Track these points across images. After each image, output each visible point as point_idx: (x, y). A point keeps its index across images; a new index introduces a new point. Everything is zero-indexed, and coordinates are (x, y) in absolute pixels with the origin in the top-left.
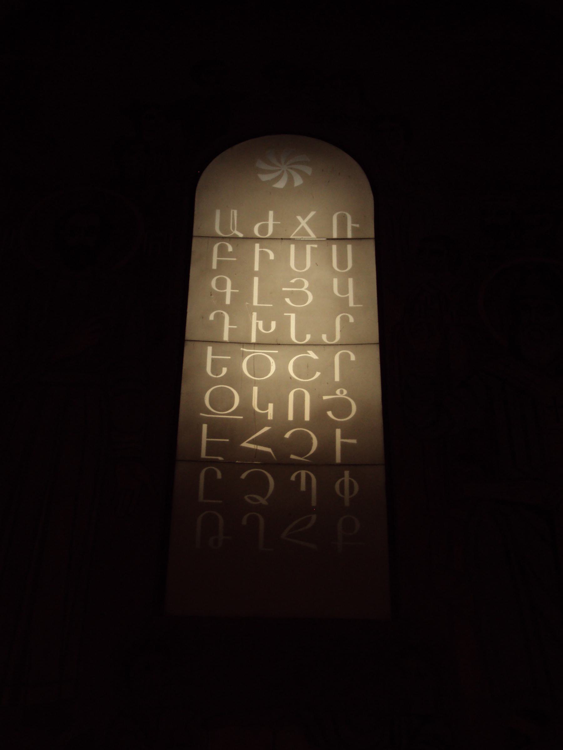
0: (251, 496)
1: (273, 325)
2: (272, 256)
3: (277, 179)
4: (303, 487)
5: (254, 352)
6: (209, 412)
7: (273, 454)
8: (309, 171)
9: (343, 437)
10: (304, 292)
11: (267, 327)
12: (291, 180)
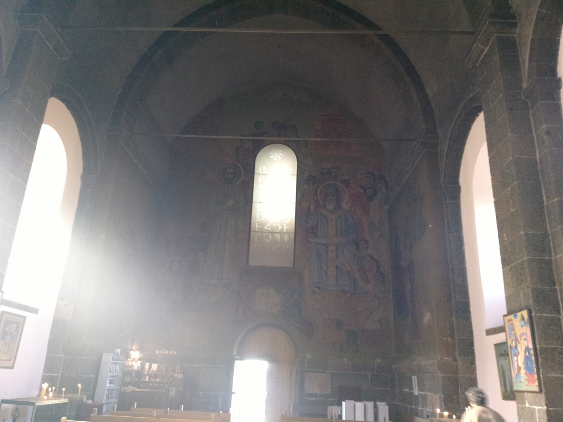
3: (275, 157)
6: (258, 220)
8: (282, 155)
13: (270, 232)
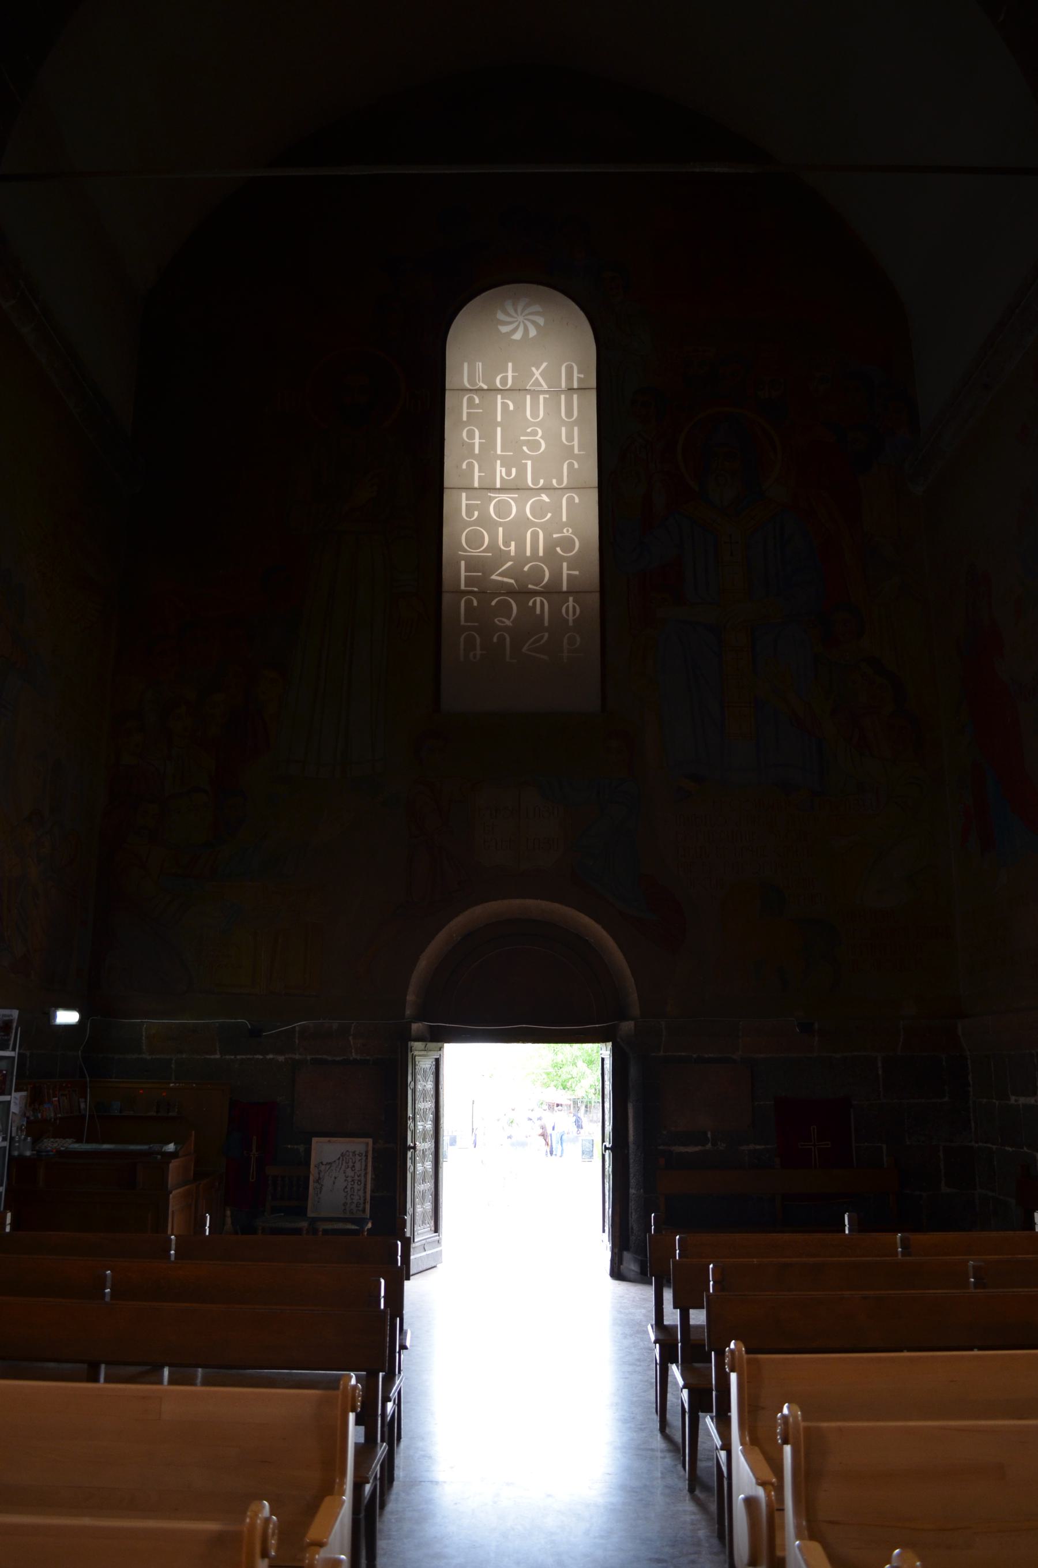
0: (500, 619)
1: (514, 471)
2: (511, 407)
3: (515, 330)
4: (538, 611)
5: (499, 497)
6: (466, 551)
7: (515, 584)
8: (541, 321)
9: (569, 569)
10: (538, 440)
11: (509, 474)
12: (526, 330)
13: (511, 592)
